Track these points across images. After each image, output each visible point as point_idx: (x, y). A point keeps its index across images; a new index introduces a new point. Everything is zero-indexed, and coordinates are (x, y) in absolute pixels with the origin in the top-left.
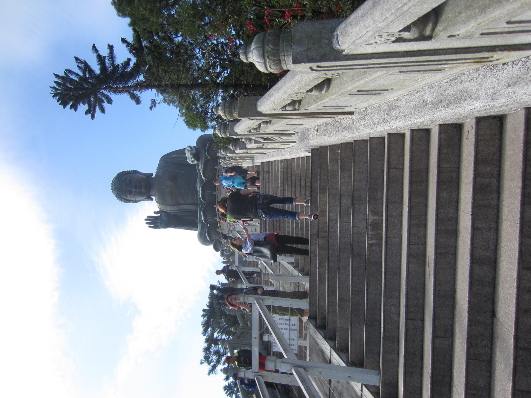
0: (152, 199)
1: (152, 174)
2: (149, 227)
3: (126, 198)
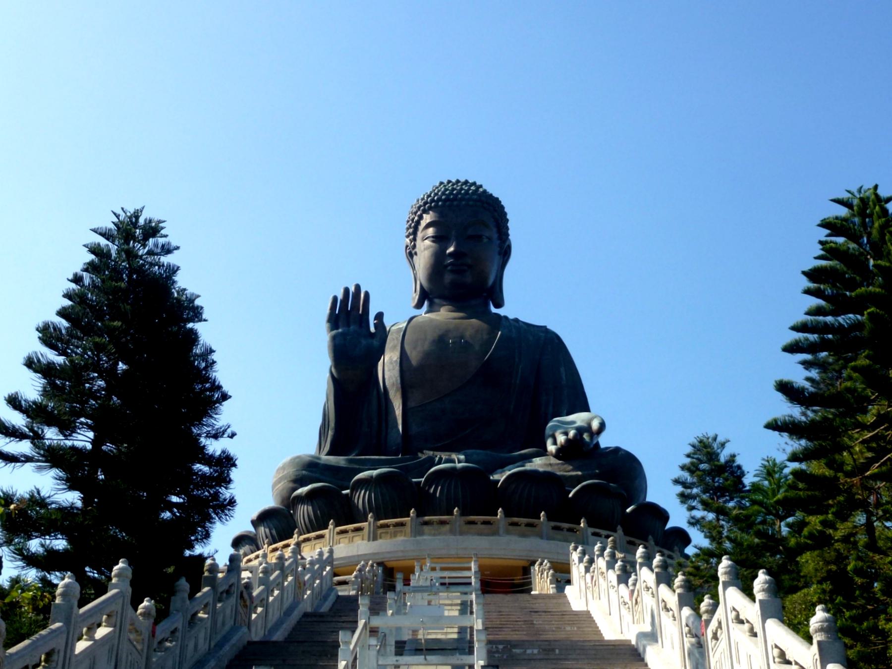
0: (419, 305)
1: (499, 304)
2: (335, 299)
3: (423, 223)
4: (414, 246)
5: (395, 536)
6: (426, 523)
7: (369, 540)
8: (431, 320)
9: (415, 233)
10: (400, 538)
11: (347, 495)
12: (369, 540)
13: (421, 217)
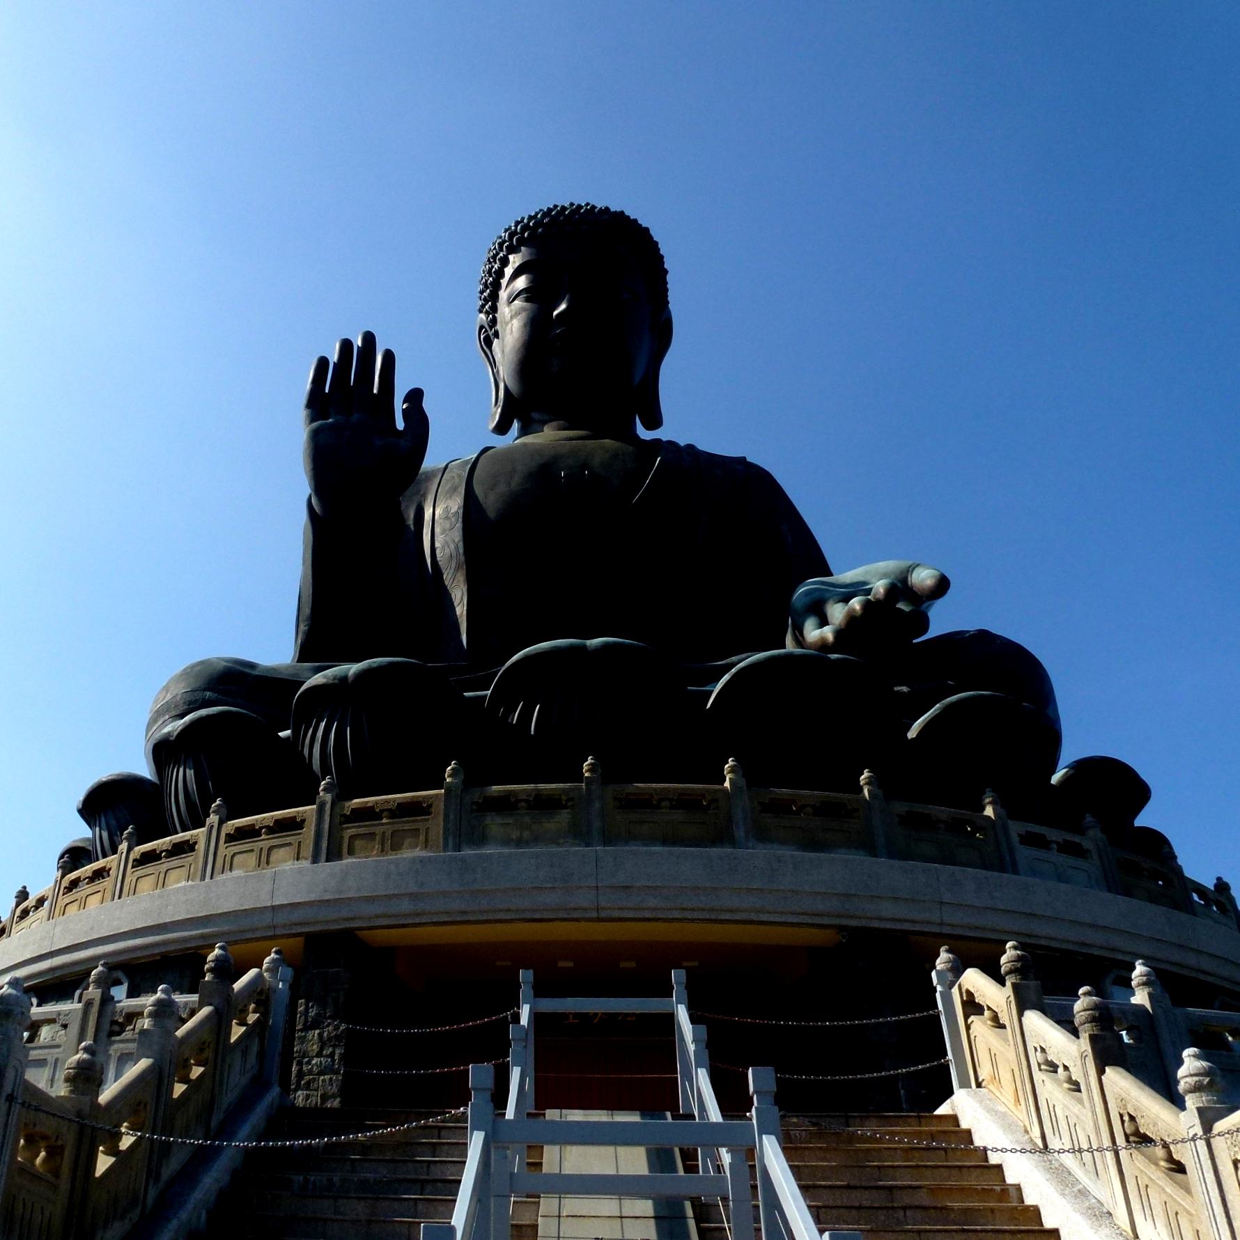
3: (509, 271)
4: (494, 322)
5: (396, 847)
6: (505, 805)
7: (315, 860)
8: (525, 445)
9: (494, 297)
10: (411, 853)
11: (288, 738)
12: (315, 860)
13: (505, 262)
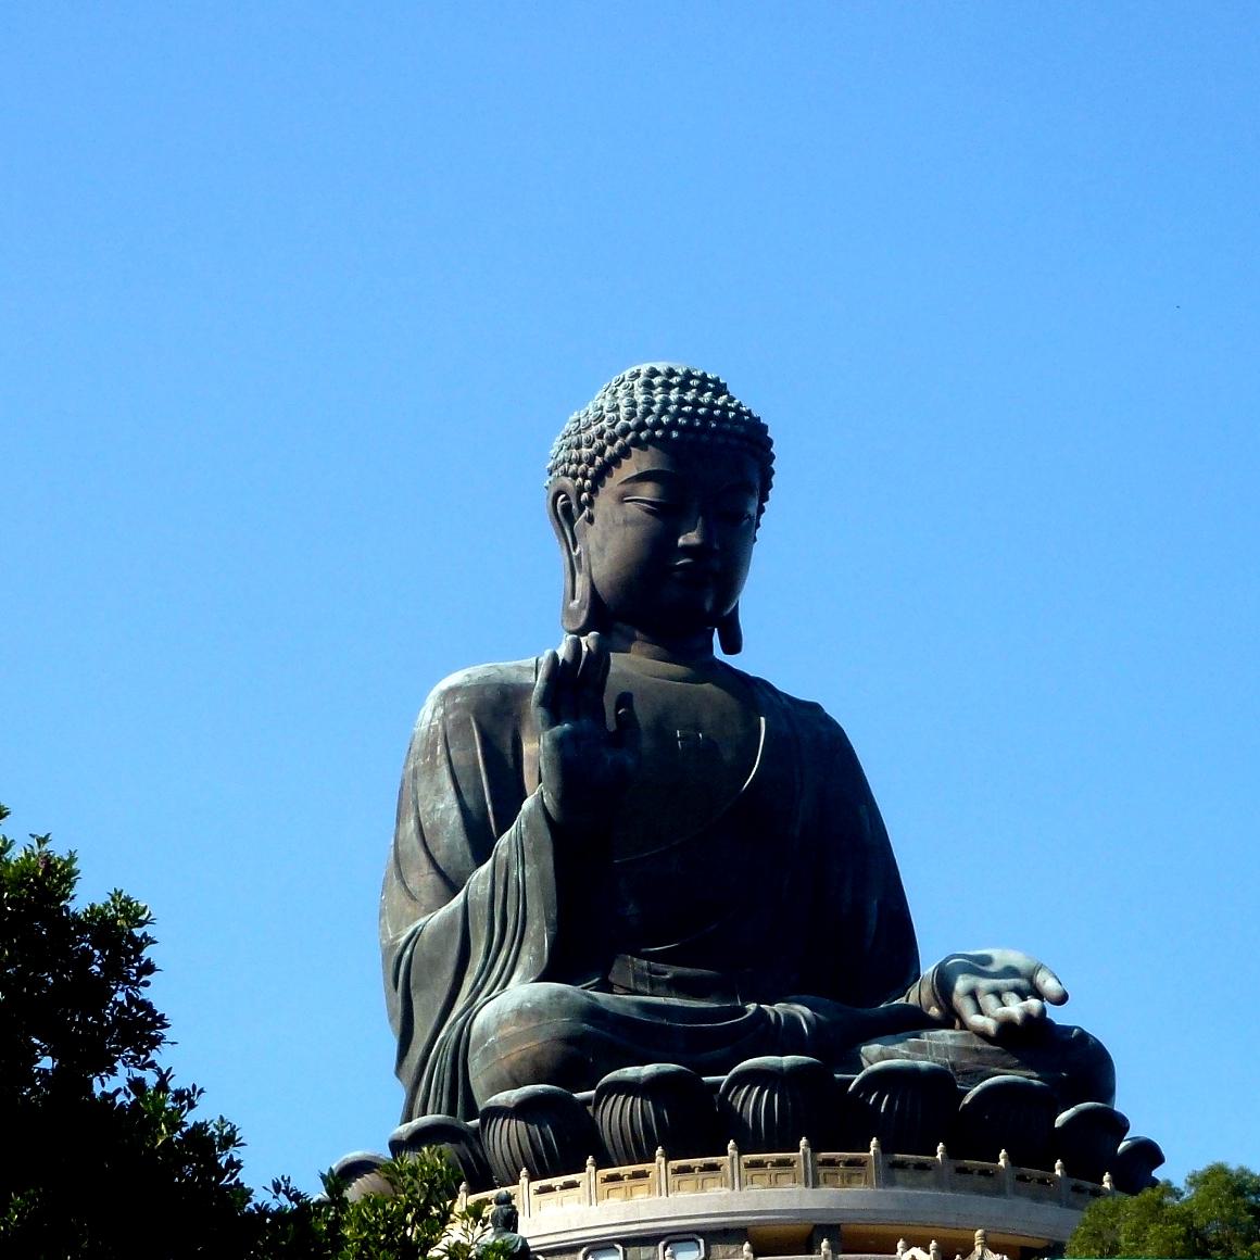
1: (733, 644)
6: (902, 1165)
13: (625, 452)
